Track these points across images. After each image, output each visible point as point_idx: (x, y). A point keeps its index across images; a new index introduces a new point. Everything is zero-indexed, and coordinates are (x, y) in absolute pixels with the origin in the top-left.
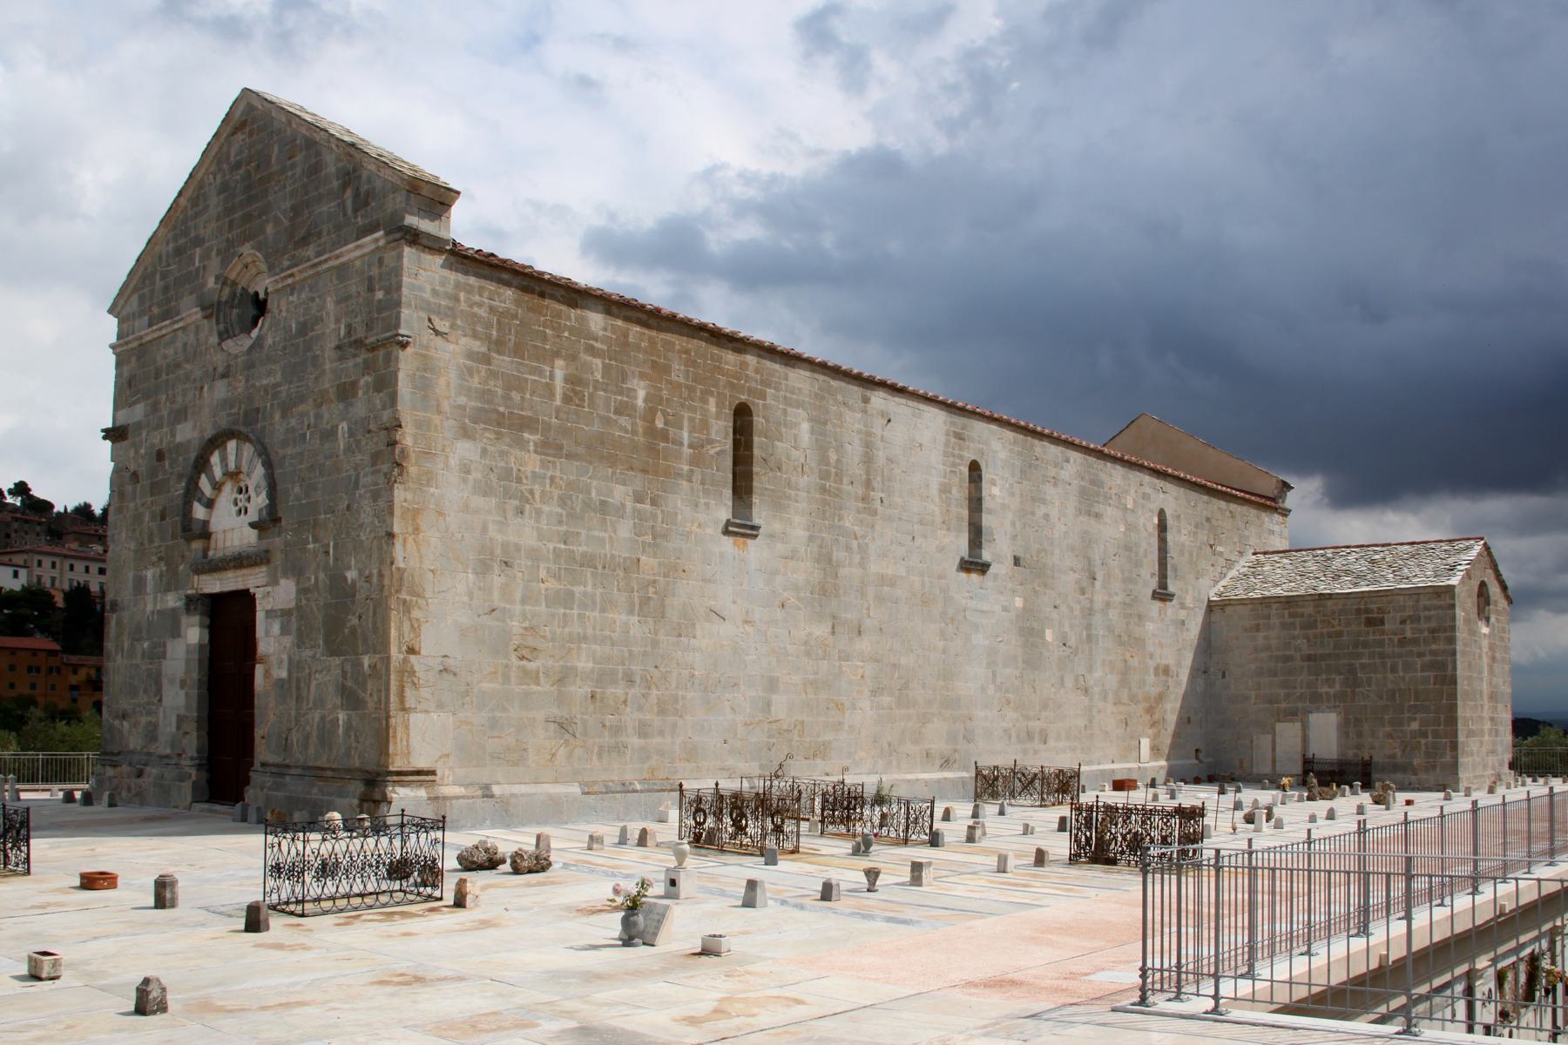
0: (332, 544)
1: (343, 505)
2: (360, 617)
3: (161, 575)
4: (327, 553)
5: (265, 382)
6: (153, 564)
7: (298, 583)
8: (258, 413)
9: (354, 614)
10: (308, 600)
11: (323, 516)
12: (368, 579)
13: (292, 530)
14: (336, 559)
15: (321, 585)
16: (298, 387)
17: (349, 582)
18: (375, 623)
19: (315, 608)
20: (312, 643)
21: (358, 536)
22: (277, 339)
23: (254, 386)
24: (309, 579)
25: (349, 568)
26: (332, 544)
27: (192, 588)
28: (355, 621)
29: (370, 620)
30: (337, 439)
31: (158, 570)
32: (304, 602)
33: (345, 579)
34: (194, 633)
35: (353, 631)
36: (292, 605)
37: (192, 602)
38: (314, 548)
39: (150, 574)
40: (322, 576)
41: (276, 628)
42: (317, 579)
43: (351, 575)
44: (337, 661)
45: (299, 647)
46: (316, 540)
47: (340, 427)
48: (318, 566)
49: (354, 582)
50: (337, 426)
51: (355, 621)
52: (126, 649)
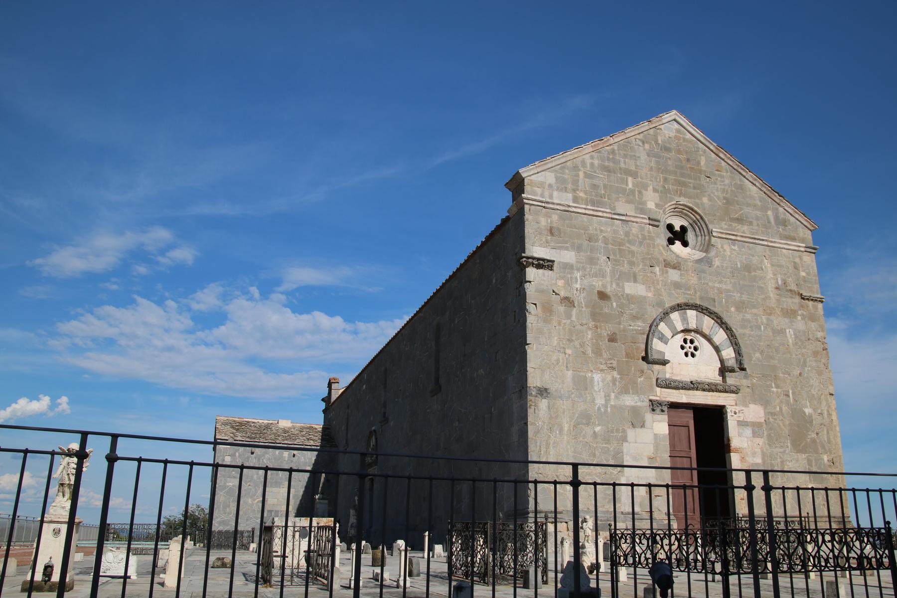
0: (791, 392)
1: (797, 372)
2: (817, 434)
3: (614, 381)
4: (788, 396)
5: (717, 285)
6: (602, 370)
7: (765, 409)
8: (715, 302)
9: (813, 432)
10: (775, 419)
11: (781, 375)
12: (821, 414)
13: (757, 377)
14: (795, 401)
15: (784, 411)
16: (748, 298)
17: (807, 414)
18: (829, 438)
19: (781, 424)
20: (782, 444)
21: (810, 391)
22: (725, 265)
23: (707, 284)
24: (775, 408)
25: (806, 407)
26: (791, 392)
27: (657, 396)
28: (814, 436)
29: (826, 436)
30: (786, 337)
31: (609, 378)
32: (771, 420)
33: (804, 413)
34: (660, 425)
35: (813, 441)
36: (762, 420)
37: (655, 406)
38: (777, 392)
39: (597, 377)
40: (785, 408)
41: (748, 432)
42: (781, 409)
43: (808, 411)
44: (804, 456)
45: (770, 445)
46: (777, 387)
47: (788, 331)
48: (781, 402)
49: (810, 416)
50: (785, 330)
51: (814, 436)
52: (566, 429)
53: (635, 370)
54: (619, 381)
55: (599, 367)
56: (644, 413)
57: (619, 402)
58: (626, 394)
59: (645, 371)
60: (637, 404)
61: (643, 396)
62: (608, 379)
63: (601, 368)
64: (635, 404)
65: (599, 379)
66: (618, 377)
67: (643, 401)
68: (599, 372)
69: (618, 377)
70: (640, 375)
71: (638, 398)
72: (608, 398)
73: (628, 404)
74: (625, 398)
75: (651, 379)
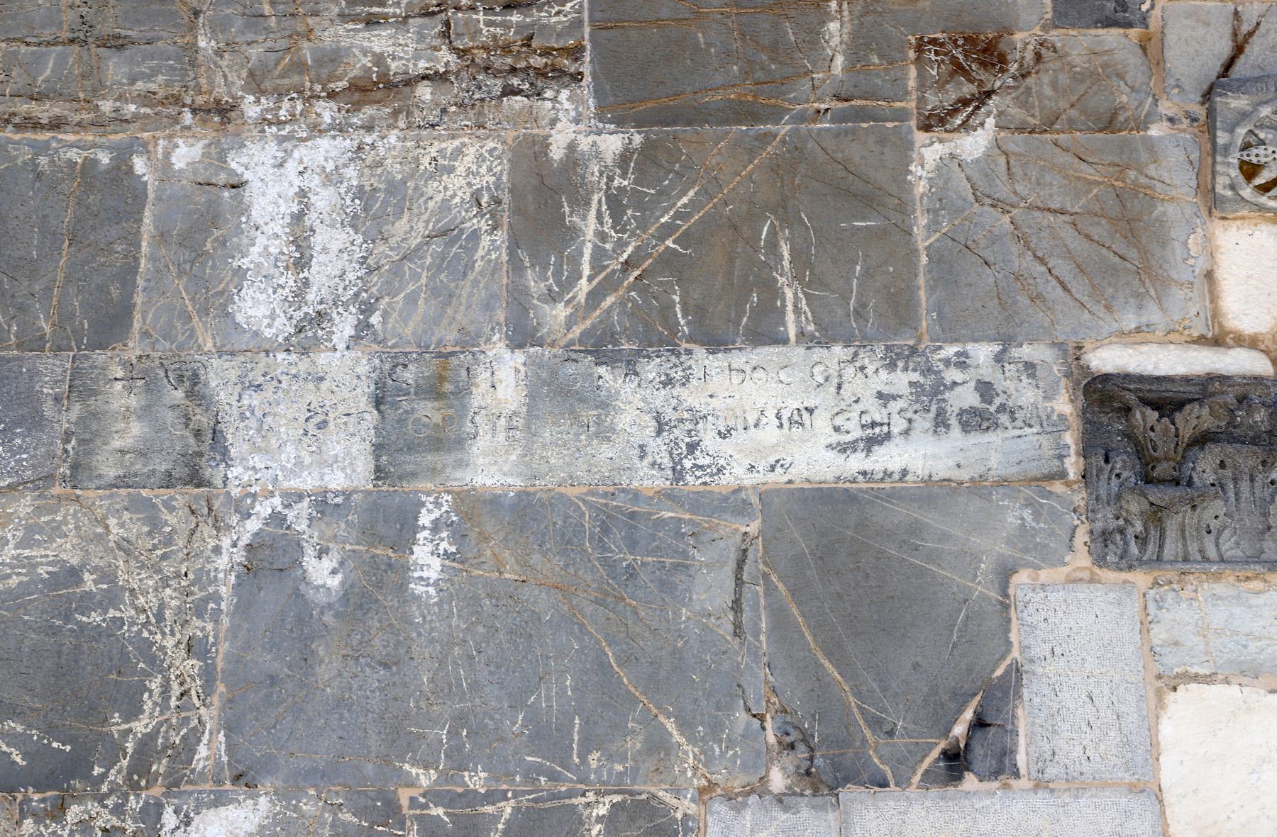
27: (1218, 341)
53: (858, 48)
54: (615, 204)
55: (335, 57)
56: (1005, 574)
57: (606, 451)
58: (716, 344)
59: (1023, 39)
60: (888, 458)
61: (983, 353)
62: (456, 186)
63: (359, 64)
64: (856, 463)
65: (323, 200)
66: (612, 143)
67: (975, 421)
68: (327, 112)
69: (612, 143)
70: (933, 100)
71: (901, 381)
72: (428, 411)
73: (736, 475)
74: (692, 397)
75: (1109, 124)
